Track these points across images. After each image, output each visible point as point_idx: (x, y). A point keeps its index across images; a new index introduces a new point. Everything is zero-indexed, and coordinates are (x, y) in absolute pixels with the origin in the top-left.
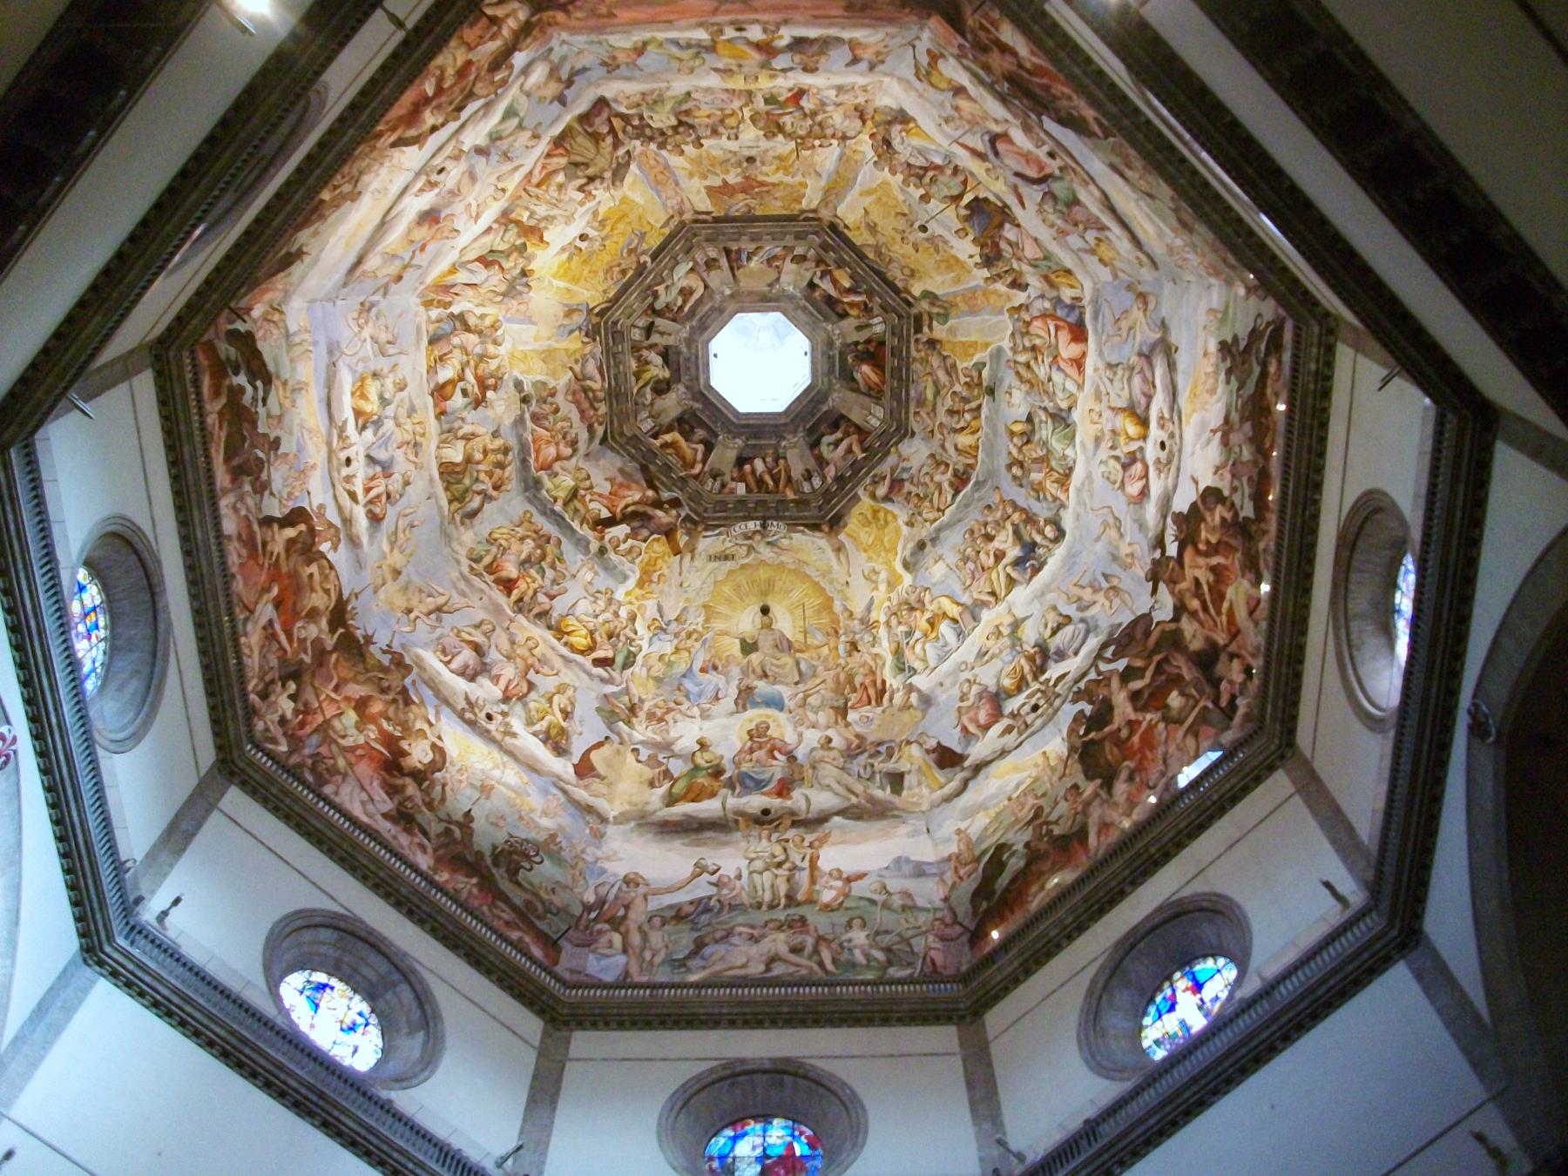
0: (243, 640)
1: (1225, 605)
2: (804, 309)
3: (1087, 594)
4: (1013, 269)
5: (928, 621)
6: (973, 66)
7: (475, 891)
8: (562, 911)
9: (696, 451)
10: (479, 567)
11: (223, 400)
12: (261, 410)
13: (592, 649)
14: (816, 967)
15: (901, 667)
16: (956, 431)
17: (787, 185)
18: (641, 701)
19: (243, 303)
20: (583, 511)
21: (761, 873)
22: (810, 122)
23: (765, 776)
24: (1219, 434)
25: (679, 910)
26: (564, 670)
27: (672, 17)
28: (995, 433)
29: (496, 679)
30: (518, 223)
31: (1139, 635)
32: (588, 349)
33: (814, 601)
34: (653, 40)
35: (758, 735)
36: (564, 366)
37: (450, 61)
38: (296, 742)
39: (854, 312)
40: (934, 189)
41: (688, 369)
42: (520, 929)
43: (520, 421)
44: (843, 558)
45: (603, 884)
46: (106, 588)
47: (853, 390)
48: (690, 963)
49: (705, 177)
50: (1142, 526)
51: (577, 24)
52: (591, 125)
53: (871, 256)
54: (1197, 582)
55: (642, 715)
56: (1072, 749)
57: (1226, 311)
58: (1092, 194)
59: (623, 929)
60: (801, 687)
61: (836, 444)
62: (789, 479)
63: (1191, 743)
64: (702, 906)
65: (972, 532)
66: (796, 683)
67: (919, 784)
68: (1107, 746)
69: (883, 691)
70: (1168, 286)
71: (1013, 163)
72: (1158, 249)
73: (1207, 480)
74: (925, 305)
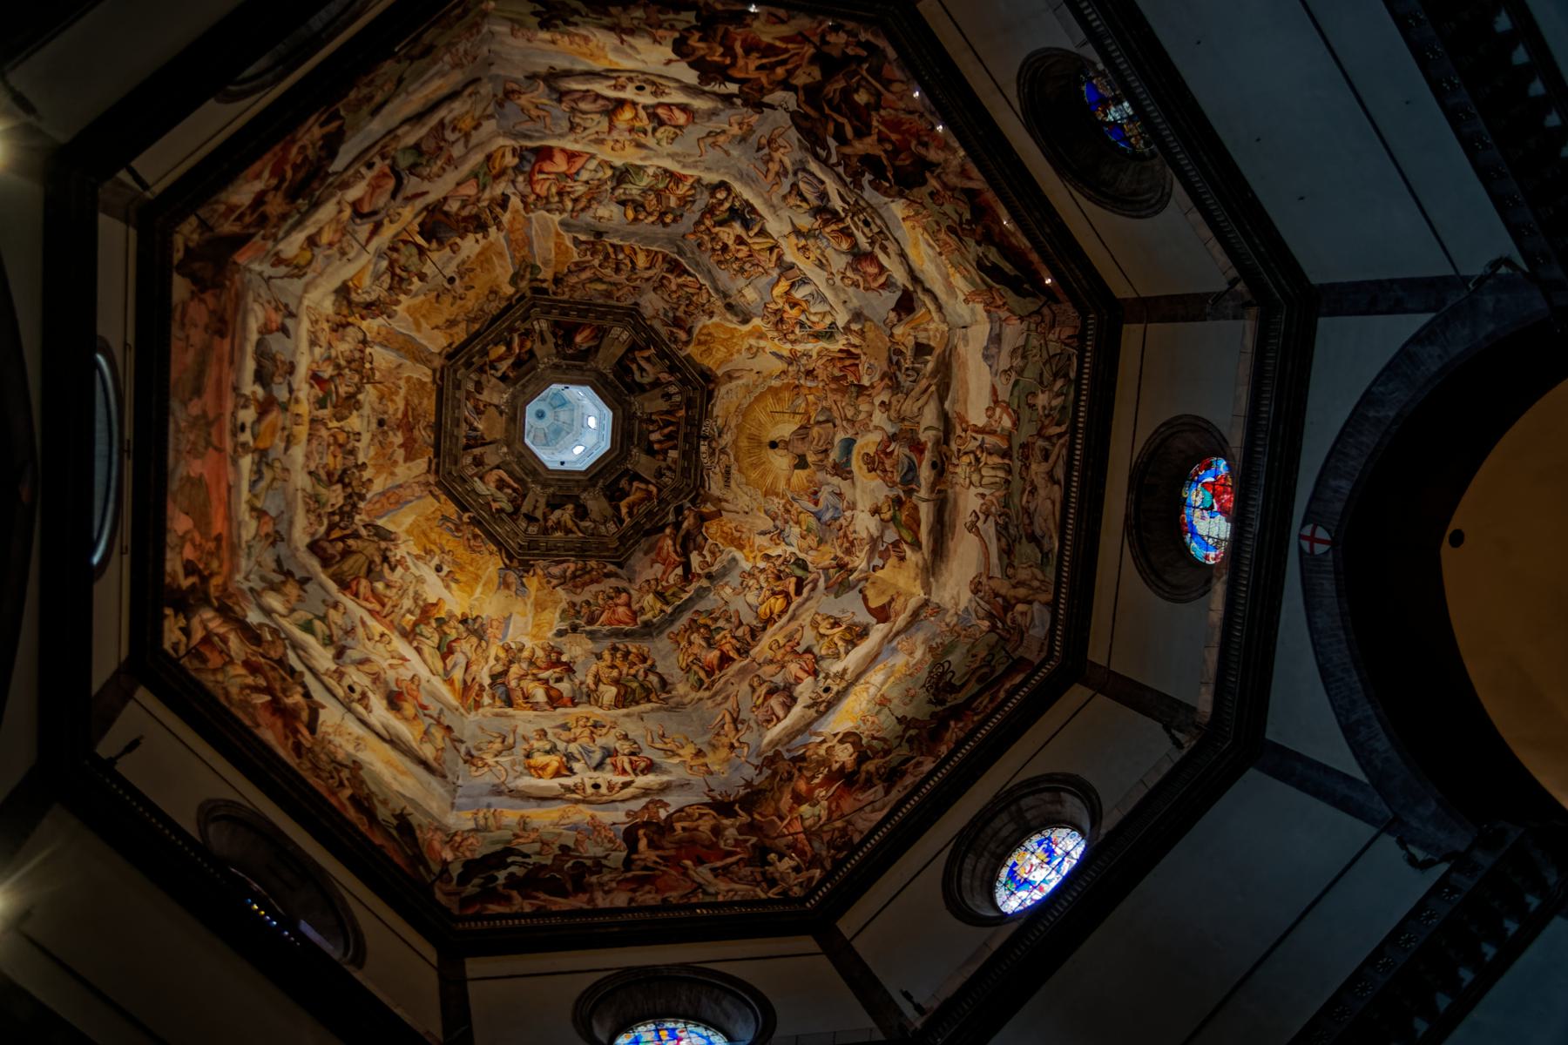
0: (720, 898)
1: (778, 43)
2: (524, 386)
3: (774, 167)
4: (488, 206)
5: (792, 308)
6: (286, 226)
7: (960, 725)
8: (992, 649)
9: (638, 488)
10: (707, 682)
11: (514, 893)
12: (531, 861)
13: (787, 595)
14: (1062, 441)
15: (829, 334)
16: (634, 268)
17: (408, 393)
18: (836, 558)
19: (436, 868)
20: (675, 589)
21: (982, 477)
22: (347, 371)
23: (906, 461)
24: (624, 37)
25: (1004, 551)
26: (800, 621)
27: (223, 485)
28: (634, 234)
29: (798, 680)
30: (416, 624)
31: (807, 124)
32: (540, 572)
33: (770, 400)
34: (248, 502)
35: (872, 464)
36: (551, 593)
37: (239, 680)
38: (815, 861)
39: (528, 345)
40: (413, 269)
41: (569, 488)
42: (998, 691)
43: (592, 635)
44: (737, 374)
45: (976, 612)
46: (642, 1019)
48: (1046, 547)
49: (395, 463)
50: (713, 113)
51: (225, 569)
52: (334, 556)
53: (477, 326)
54: (760, 68)
55: (847, 559)
56: (901, 195)
57: (511, 20)
58: (407, 133)
59: (1013, 602)
60: (838, 422)
61: (642, 370)
62: (668, 412)
63: (896, 87)
64: (1002, 531)
65: (719, 262)
66: (835, 426)
67: (926, 330)
68: (898, 163)
69: (848, 352)
70: (494, 70)
71: (382, 200)
72: (457, 77)
73: (667, 52)
74: (523, 284)
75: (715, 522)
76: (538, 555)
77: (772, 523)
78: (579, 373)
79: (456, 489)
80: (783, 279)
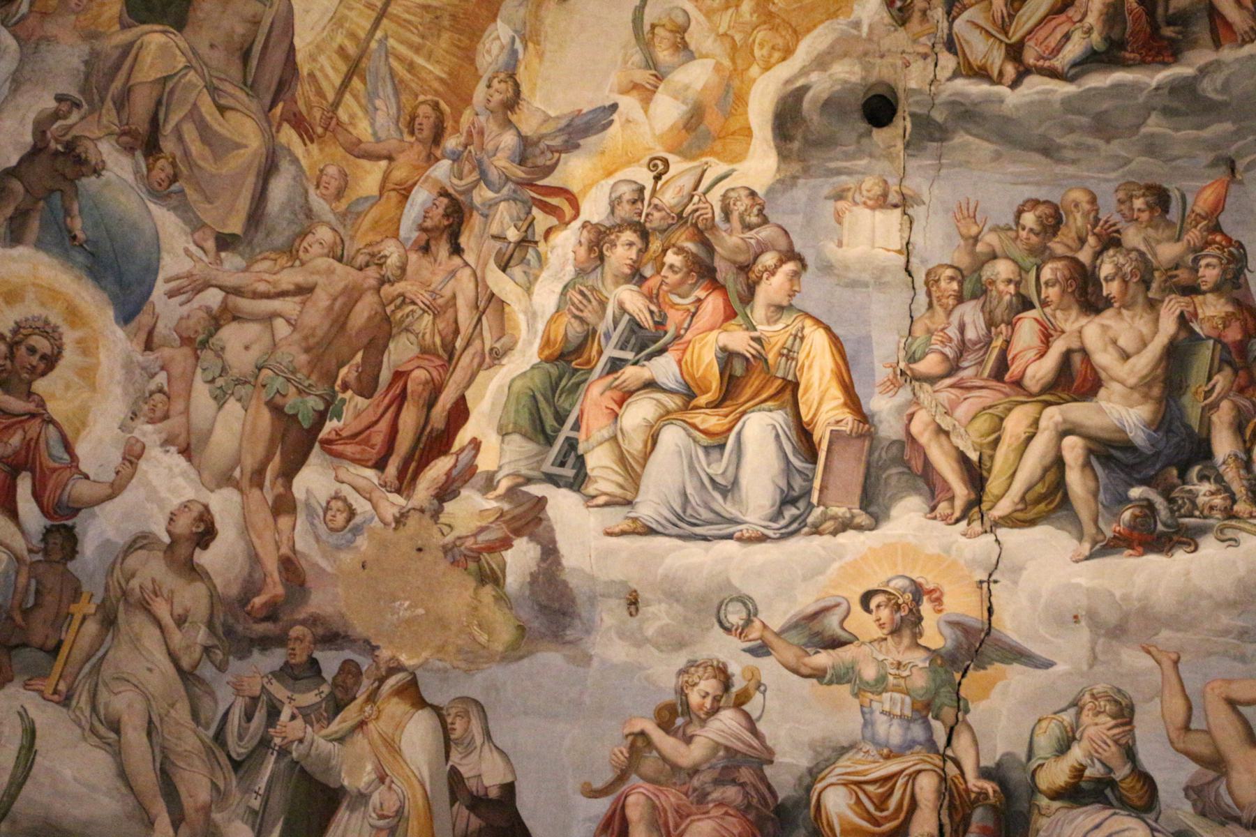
5: (727, 357)
60: (232, 260)
65: (1053, 222)
80: (848, 421)
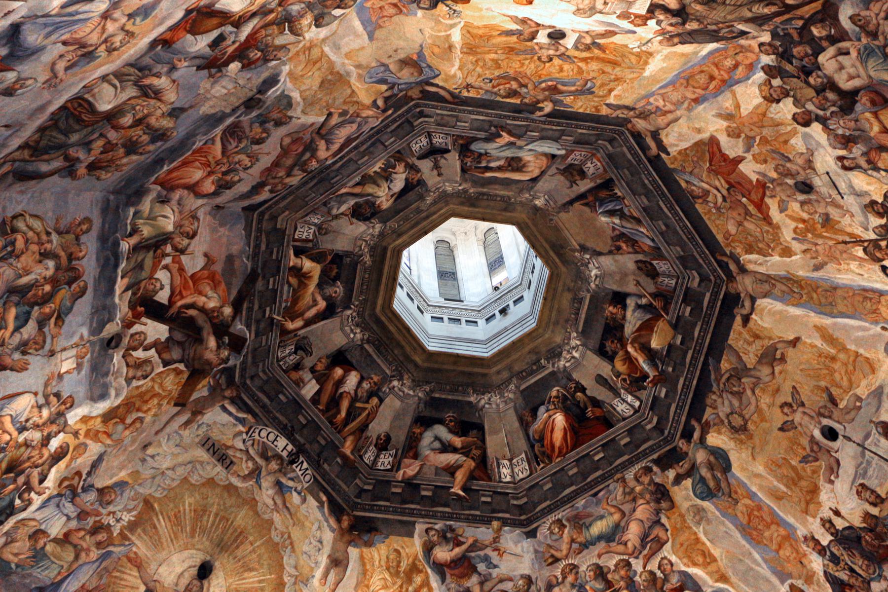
9: (316, 305)
20: (144, 274)
39: (620, 366)
41: (406, 219)
43: (214, 120)
44: (332, 577)
47: (521, 420)
49: (733, 134)
53: (725, 365)
61: (447, 448)
62: (364, 427)
74: (701, 456)
75: (175, 394)
76: (387, 126)
77: (99, 484)
78: (517, 368)
79: (588, 128)
